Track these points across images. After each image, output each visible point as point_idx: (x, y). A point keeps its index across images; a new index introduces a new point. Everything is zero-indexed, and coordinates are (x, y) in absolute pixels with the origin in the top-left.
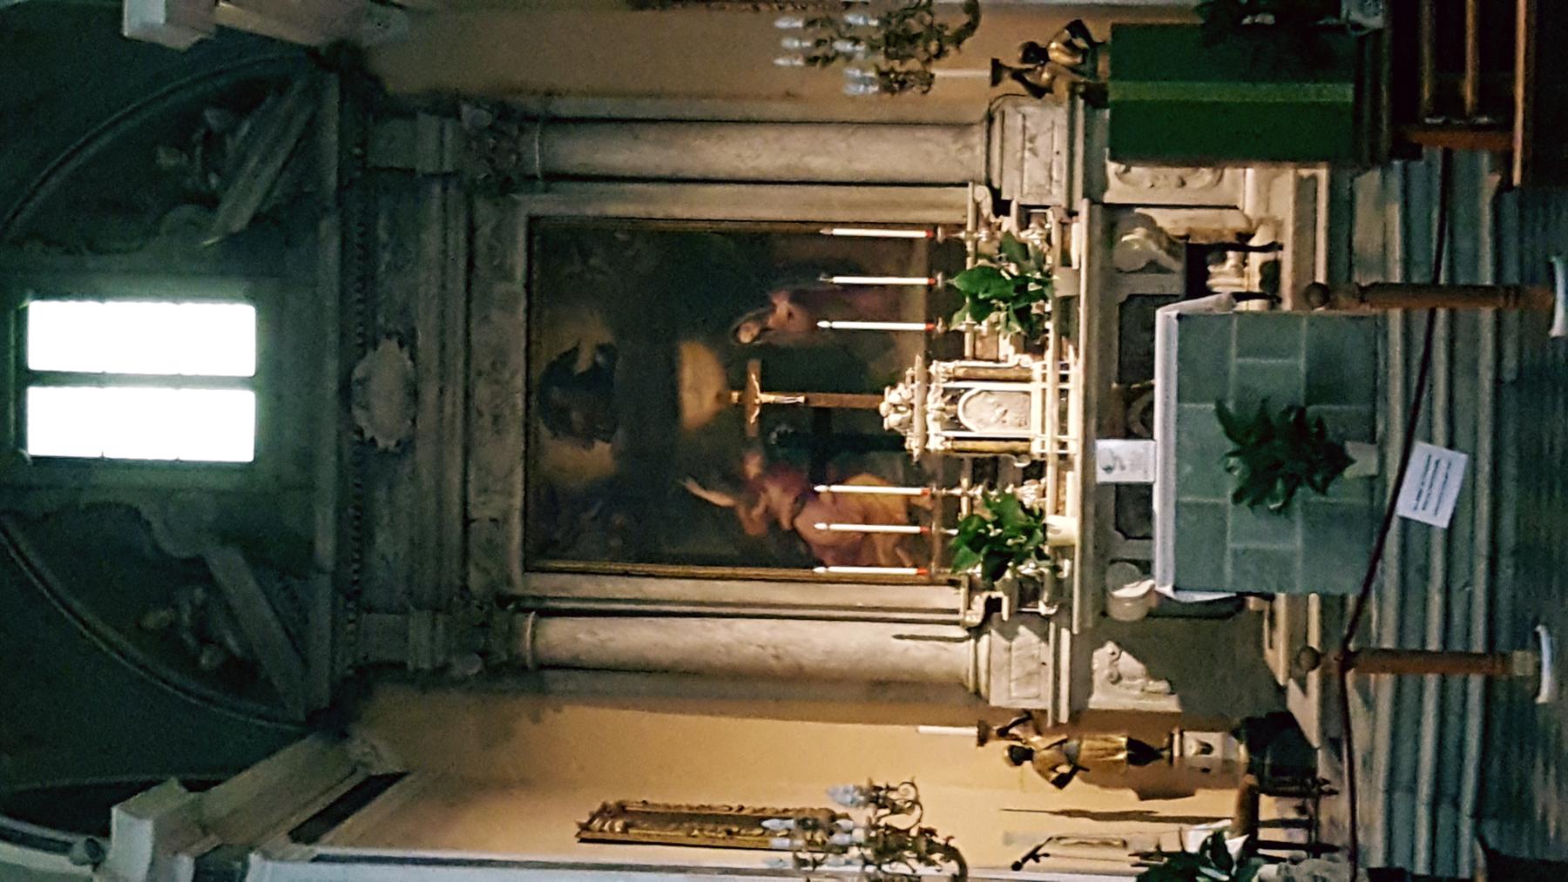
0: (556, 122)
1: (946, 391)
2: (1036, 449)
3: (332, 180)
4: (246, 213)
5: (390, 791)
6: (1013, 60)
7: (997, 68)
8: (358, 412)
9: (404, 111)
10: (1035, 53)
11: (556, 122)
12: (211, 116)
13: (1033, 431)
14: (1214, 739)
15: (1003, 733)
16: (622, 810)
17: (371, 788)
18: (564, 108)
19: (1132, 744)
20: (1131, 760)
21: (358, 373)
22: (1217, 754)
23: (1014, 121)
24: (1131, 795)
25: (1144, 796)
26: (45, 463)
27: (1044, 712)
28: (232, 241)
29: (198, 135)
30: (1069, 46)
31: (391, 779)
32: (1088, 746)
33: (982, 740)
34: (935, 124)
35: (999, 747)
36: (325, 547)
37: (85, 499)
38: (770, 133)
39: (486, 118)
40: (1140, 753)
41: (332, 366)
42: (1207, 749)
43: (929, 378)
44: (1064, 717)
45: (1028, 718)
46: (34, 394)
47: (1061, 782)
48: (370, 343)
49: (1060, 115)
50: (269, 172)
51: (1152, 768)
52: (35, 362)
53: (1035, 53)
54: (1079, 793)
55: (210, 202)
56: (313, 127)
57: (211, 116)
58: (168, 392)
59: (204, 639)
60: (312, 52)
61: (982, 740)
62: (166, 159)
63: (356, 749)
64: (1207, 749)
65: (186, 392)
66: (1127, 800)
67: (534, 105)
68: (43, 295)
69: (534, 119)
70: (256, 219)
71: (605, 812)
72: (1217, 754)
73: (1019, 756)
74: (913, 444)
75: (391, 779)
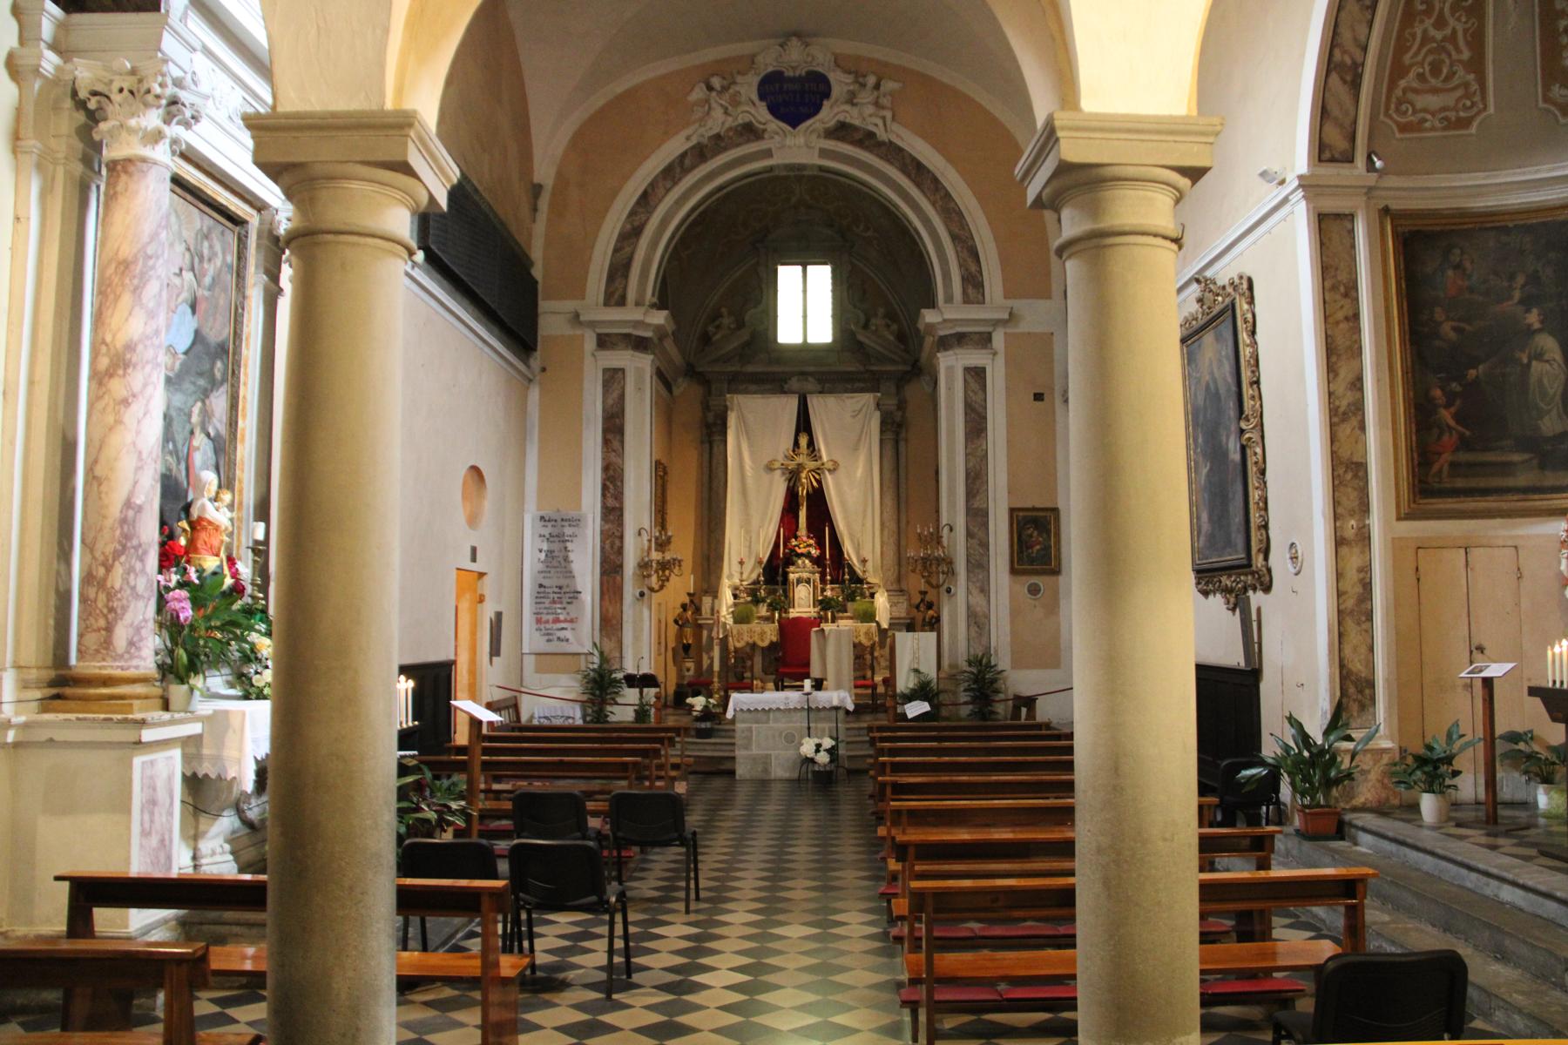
0: (897, 442)
1: (809, 579)
2: (791, 610)
3: (874, 368)
4: (866, 341)
5: (666, 392)
6: (928, 598)
7: (924, 593)
8: (794, 379)
9: (899, 388)
10: (930, 606)
11: (897, 442)
12: (895, 327)
13: (797, 609)
14: (692, 672)
15: (692, 601)
16: (666, 473)
17: (668, 385)
18: (902, 444)
19: (689, 645)
20: (684, 644)
21: (810, 379)
22: (687, 674)
23: (902, 599)
24: (674, 645)
25: (673, 649)
26: (776, 272)
27: (701, 615)
28: (853, 334)
29: (889, 322)
30: (933, 617)
31: (670, 391)
32: (688, 631)
33: (689, 594)
34: (899, 572)
35: (687, 600)
36: (750, 369)
37: (764, 286)
38: (895, 517)
39: (898, 419)
40: (686, 648)
41: (812, 369)
42: (688, 670)
43: (814, 573)
44: (700, 622)
45: (698, 610)
46: (799, 268)
47: (676, 622)
48: (820, 381)
49: (903, 615)
50: (878, 348)
51: (681, 652)
52: (810, 268)
53: (930, 606)
54: (673, 629)
55: (866, 326)
56: (893, 362)
57: (895, 327)
58: (801, 314)
59: (718, 327)
60: (917, 361)
61: (689, 594)
62: (881, 311)
63: (680, 380)
64: (688, 670)
65: (801, 319)
66: (672, 644)
67: (903, 435)
68: (833, 272)
69: (898, 434)
70: (860, 344)
71: (665, 469)
72: (687, 674)
73: (684, 607)
74: (792, 568)
75: (670, 391)
